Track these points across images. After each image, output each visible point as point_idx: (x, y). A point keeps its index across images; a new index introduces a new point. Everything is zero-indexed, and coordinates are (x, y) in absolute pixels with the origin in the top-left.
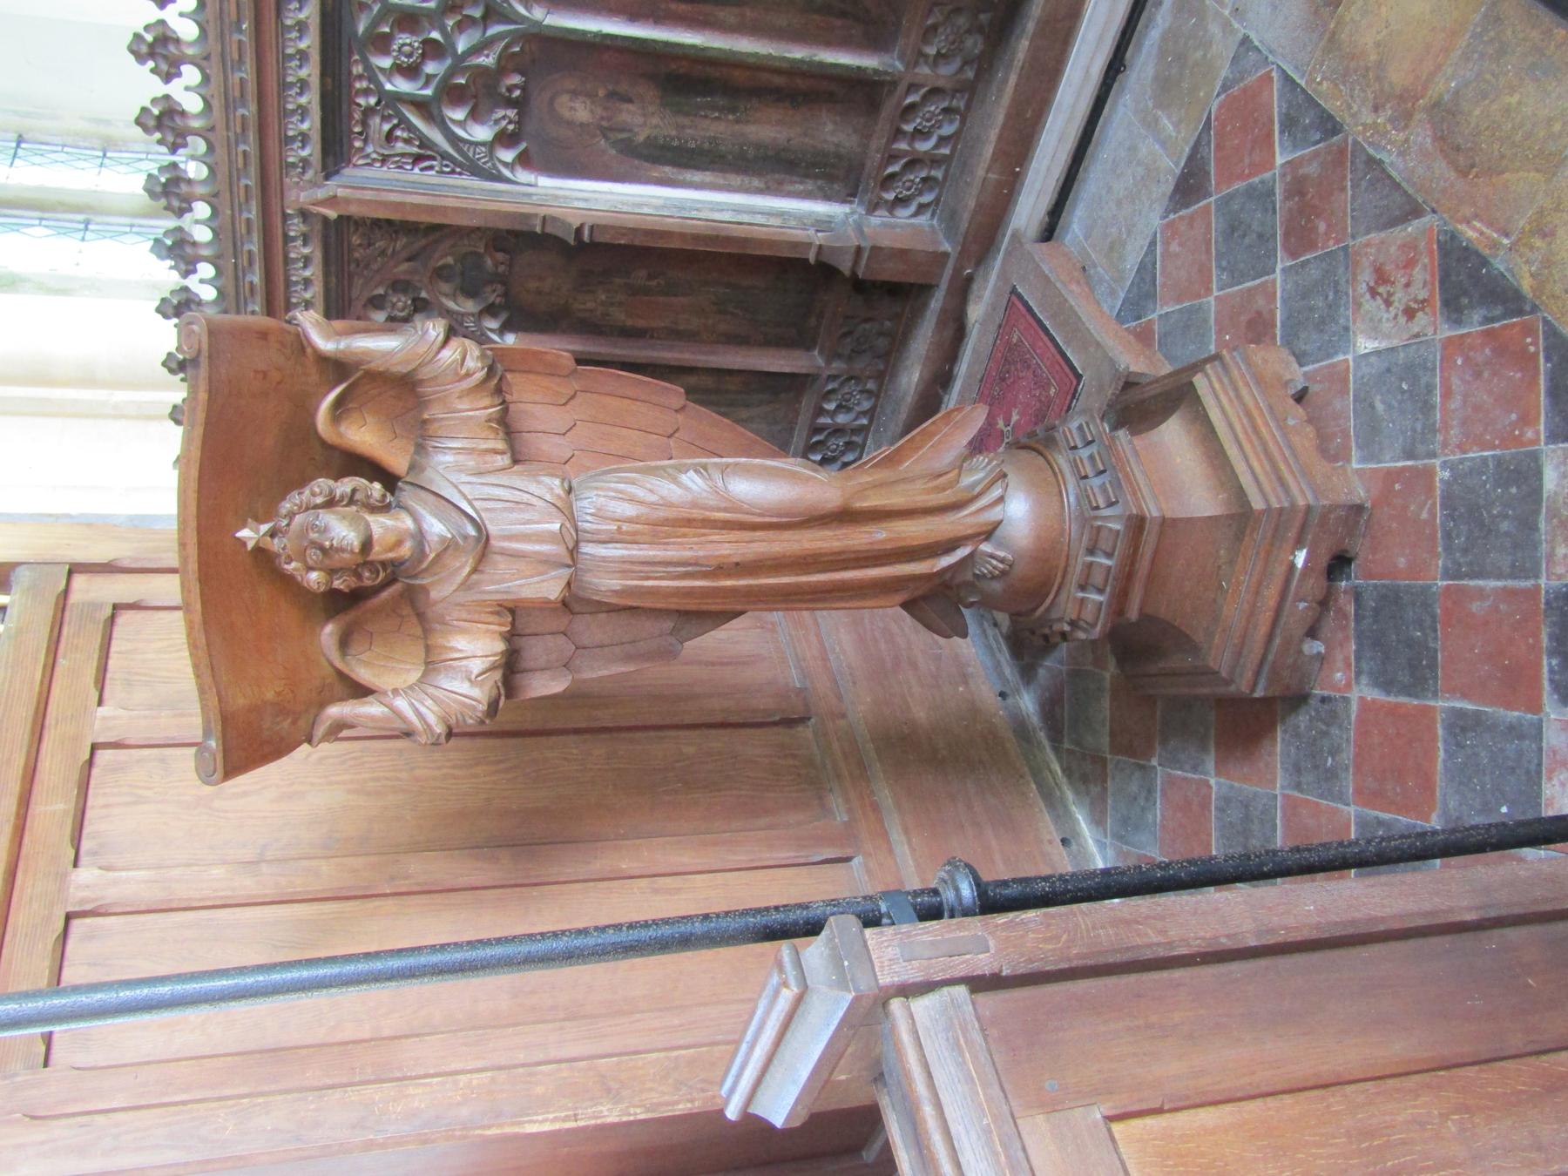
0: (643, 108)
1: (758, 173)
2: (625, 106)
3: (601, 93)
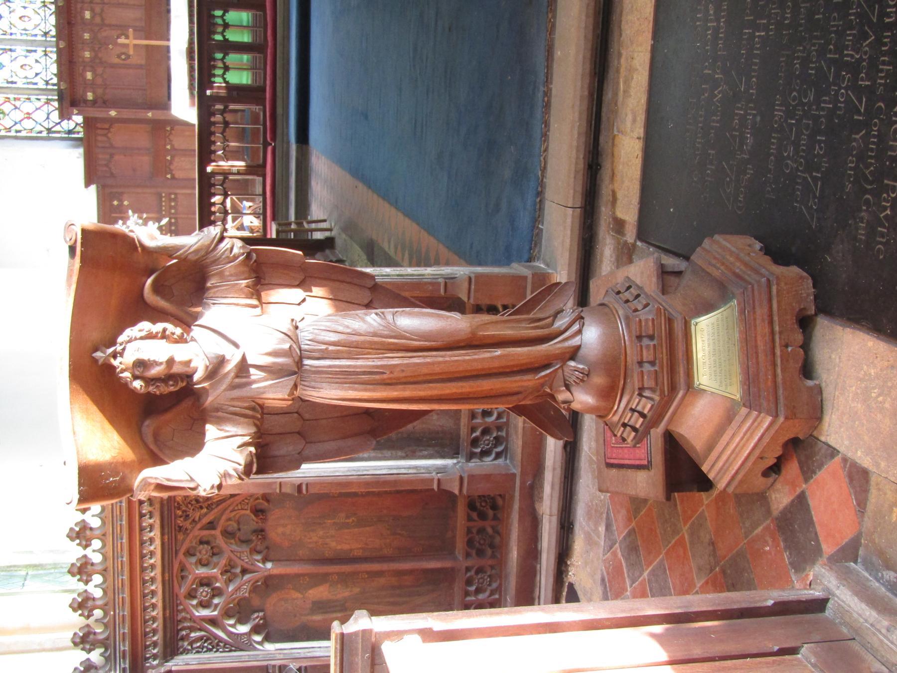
1: (401, 448)
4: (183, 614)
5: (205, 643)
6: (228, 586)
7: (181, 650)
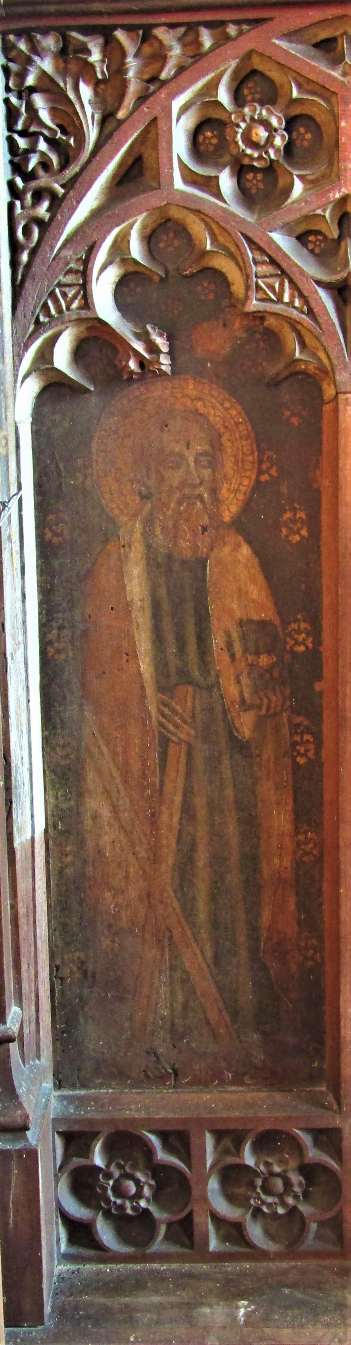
4: (176, 51)
5: (52, 142)
6: (288, 229)
7: (23, 46)
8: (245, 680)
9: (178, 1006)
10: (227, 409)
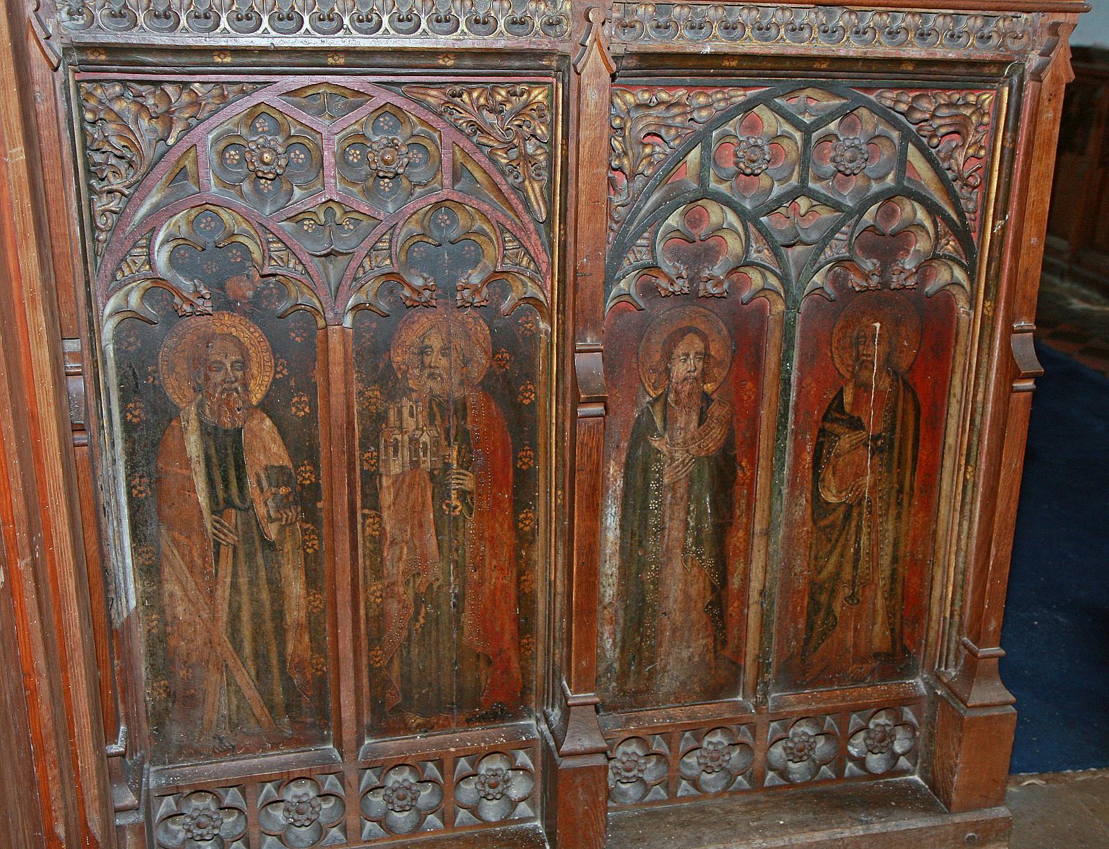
0: (693, 438)
2: (695, 417)
3: (709, 387)
8: (270, 503)
9: (234, 707)
10: (252, 333)
